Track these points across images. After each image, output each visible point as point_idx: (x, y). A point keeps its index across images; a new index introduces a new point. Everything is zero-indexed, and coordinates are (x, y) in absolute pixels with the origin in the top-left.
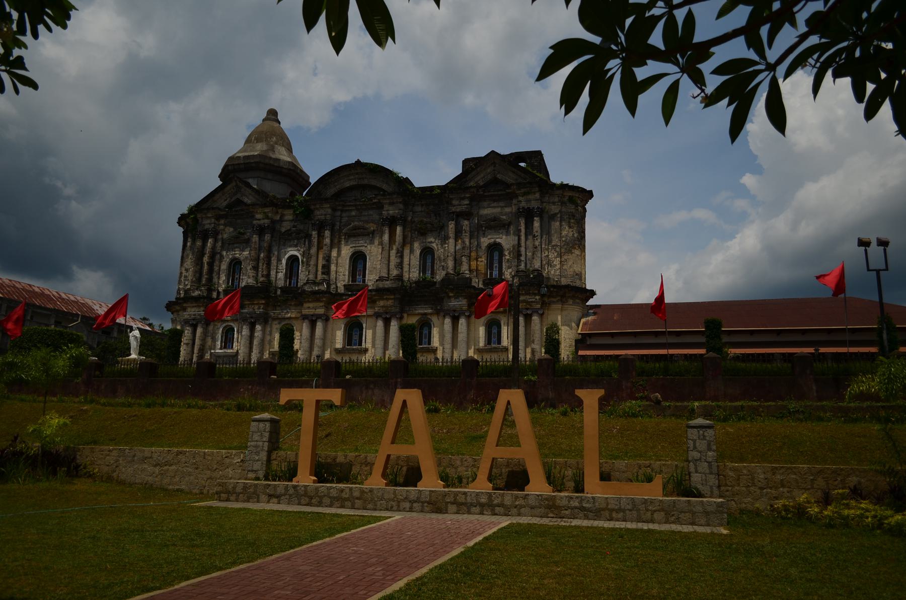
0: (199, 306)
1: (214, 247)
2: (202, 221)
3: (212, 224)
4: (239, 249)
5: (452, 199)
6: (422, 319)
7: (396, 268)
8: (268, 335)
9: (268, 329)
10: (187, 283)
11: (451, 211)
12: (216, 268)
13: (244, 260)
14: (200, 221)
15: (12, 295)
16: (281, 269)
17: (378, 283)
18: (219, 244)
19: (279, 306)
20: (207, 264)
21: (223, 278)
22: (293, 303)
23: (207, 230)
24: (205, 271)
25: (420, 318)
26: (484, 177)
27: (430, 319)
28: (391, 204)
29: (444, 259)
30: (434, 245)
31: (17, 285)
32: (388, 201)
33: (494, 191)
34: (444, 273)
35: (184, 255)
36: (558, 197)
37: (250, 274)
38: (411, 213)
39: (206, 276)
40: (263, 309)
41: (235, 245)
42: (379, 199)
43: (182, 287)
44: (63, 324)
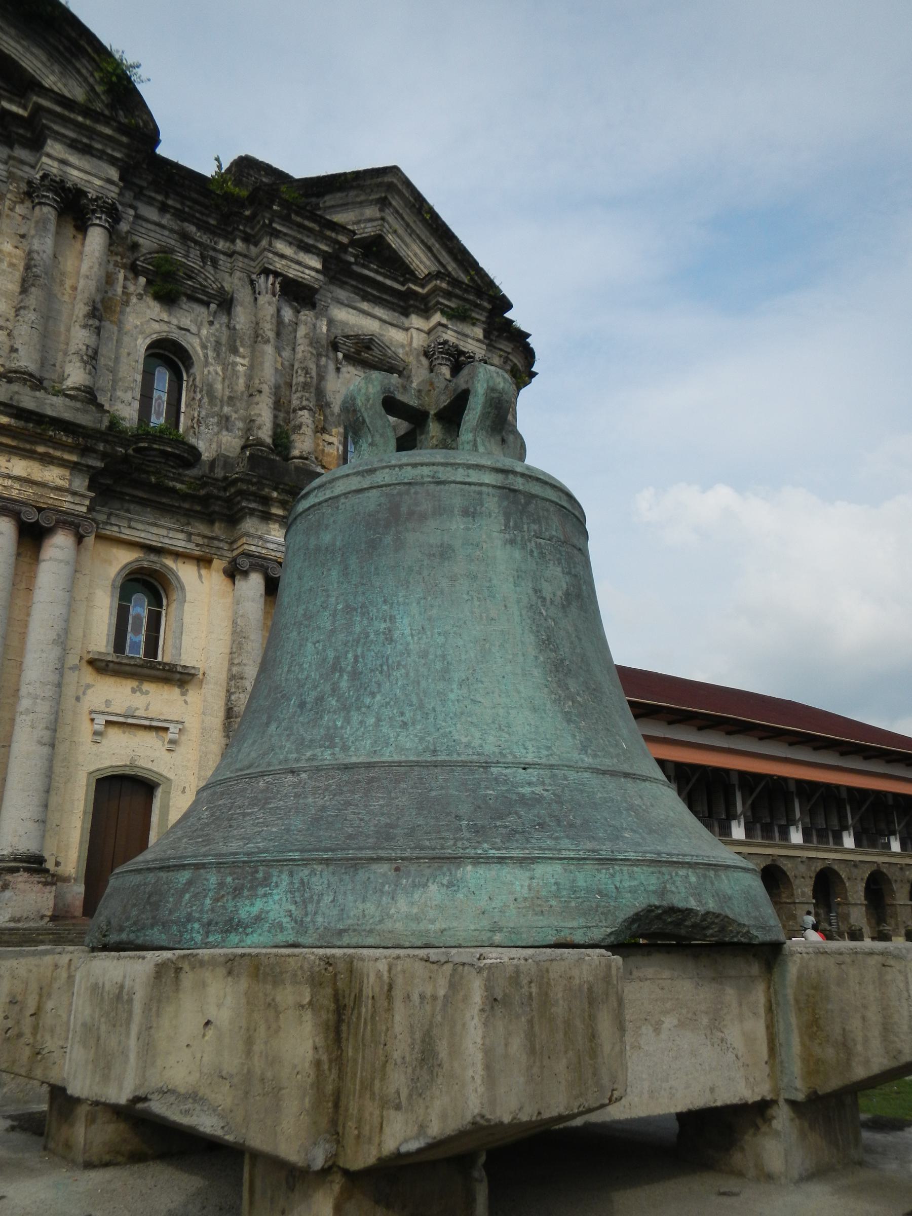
5: (276, 234)
6: (146, 564)
7: (85, 363)
11: (271, 267)
17: (15, 387)
25: (137, 560)
26: (358, 222)
27: (171, 570)
28: (74, 145)
29: (231, 398)
30: (196, 342)
32: (71, 134)
33: (377, 272)
34: (231, 442)
36: (500, 356)
38: (132, 212)
42: (38, 108)
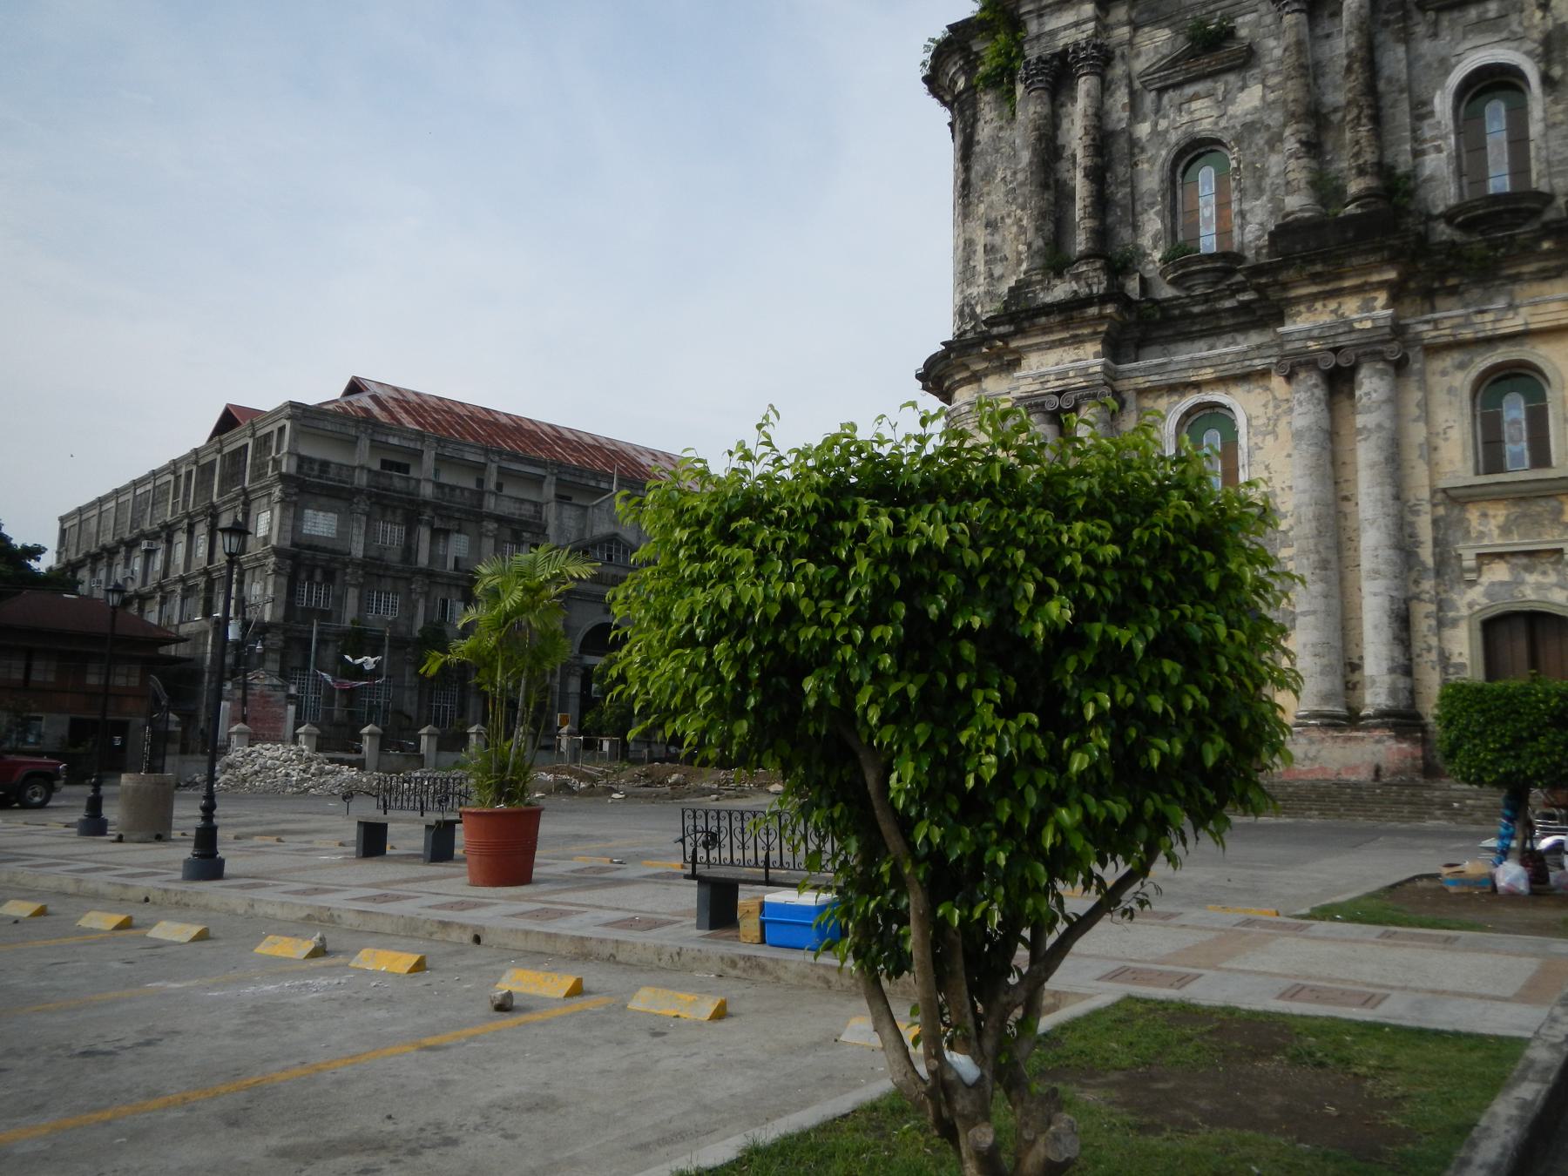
0: (1077, 341)
1: (1099, 115)
2: (1041, 25)
3: (1085, 22)
4: (1206, 102)
8: (1417, 420)
9: (1414, 396)
10: (998, 271)
12: (1121, 194)
13: (1238, 140)
14: (1033, 27)
15: (445, 429)
16: (1435, 138)
18: (1121, 97)
19: (1453, 291)
20: (1086, 176)
21: (1152, 224)
22: (1526, 269)
23: (1065, 51)
24: (1079, 204)
31: (457, 410)
35: (973, 175)
37: (1291, 176)
39: (1089, 223)
40: (1384, 308)
41: (1189, 90)
43: (982, 289)
44: (574, 501)
